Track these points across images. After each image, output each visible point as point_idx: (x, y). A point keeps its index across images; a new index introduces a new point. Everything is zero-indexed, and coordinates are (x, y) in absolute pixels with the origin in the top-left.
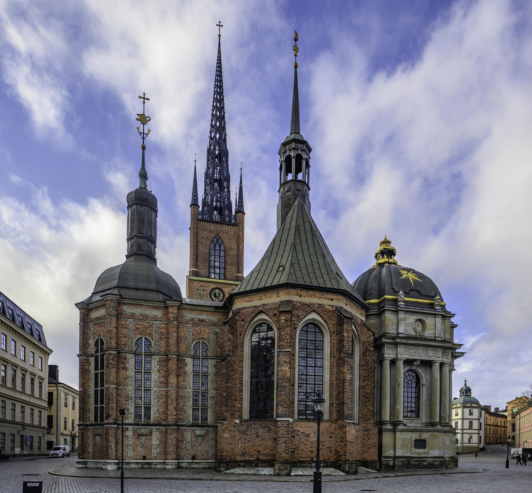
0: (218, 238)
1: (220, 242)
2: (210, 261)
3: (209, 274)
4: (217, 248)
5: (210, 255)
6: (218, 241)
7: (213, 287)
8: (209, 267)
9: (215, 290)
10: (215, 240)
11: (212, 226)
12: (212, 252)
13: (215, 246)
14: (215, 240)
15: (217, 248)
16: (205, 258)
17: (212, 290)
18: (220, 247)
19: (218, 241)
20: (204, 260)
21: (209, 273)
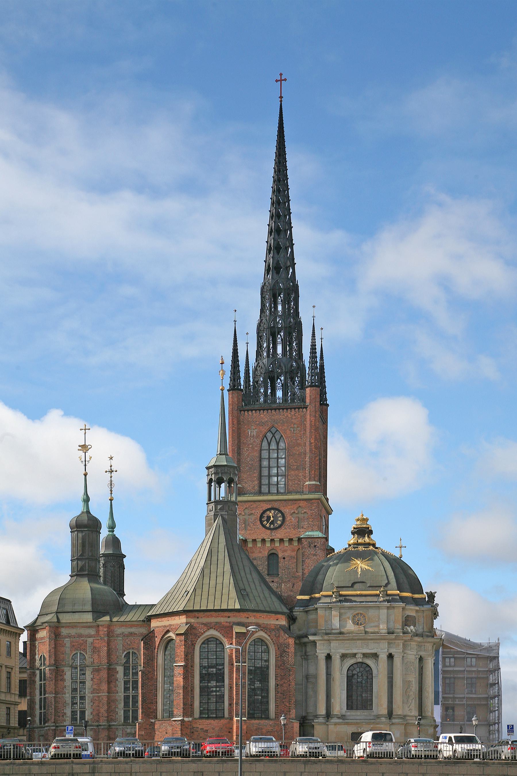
0: (273, 430)
1: (277, 436)
2: (261, 467)
3: (260, 487)
4: (273, 446)
5: (261, 459)
6: (274, 436)
7: (264, 509)
8: (260, 476)
9: (268, 512)
10: (269, 435)
11: (264, 416)
12: (265, 454)
13: (269, 444)
14: (269, 435)
15: (273, 446)
16: (252, 465)
17: (264, 512)
18: (278, 443)
19: (274, 436)
20: (250, 468)
21: (260, 485)
